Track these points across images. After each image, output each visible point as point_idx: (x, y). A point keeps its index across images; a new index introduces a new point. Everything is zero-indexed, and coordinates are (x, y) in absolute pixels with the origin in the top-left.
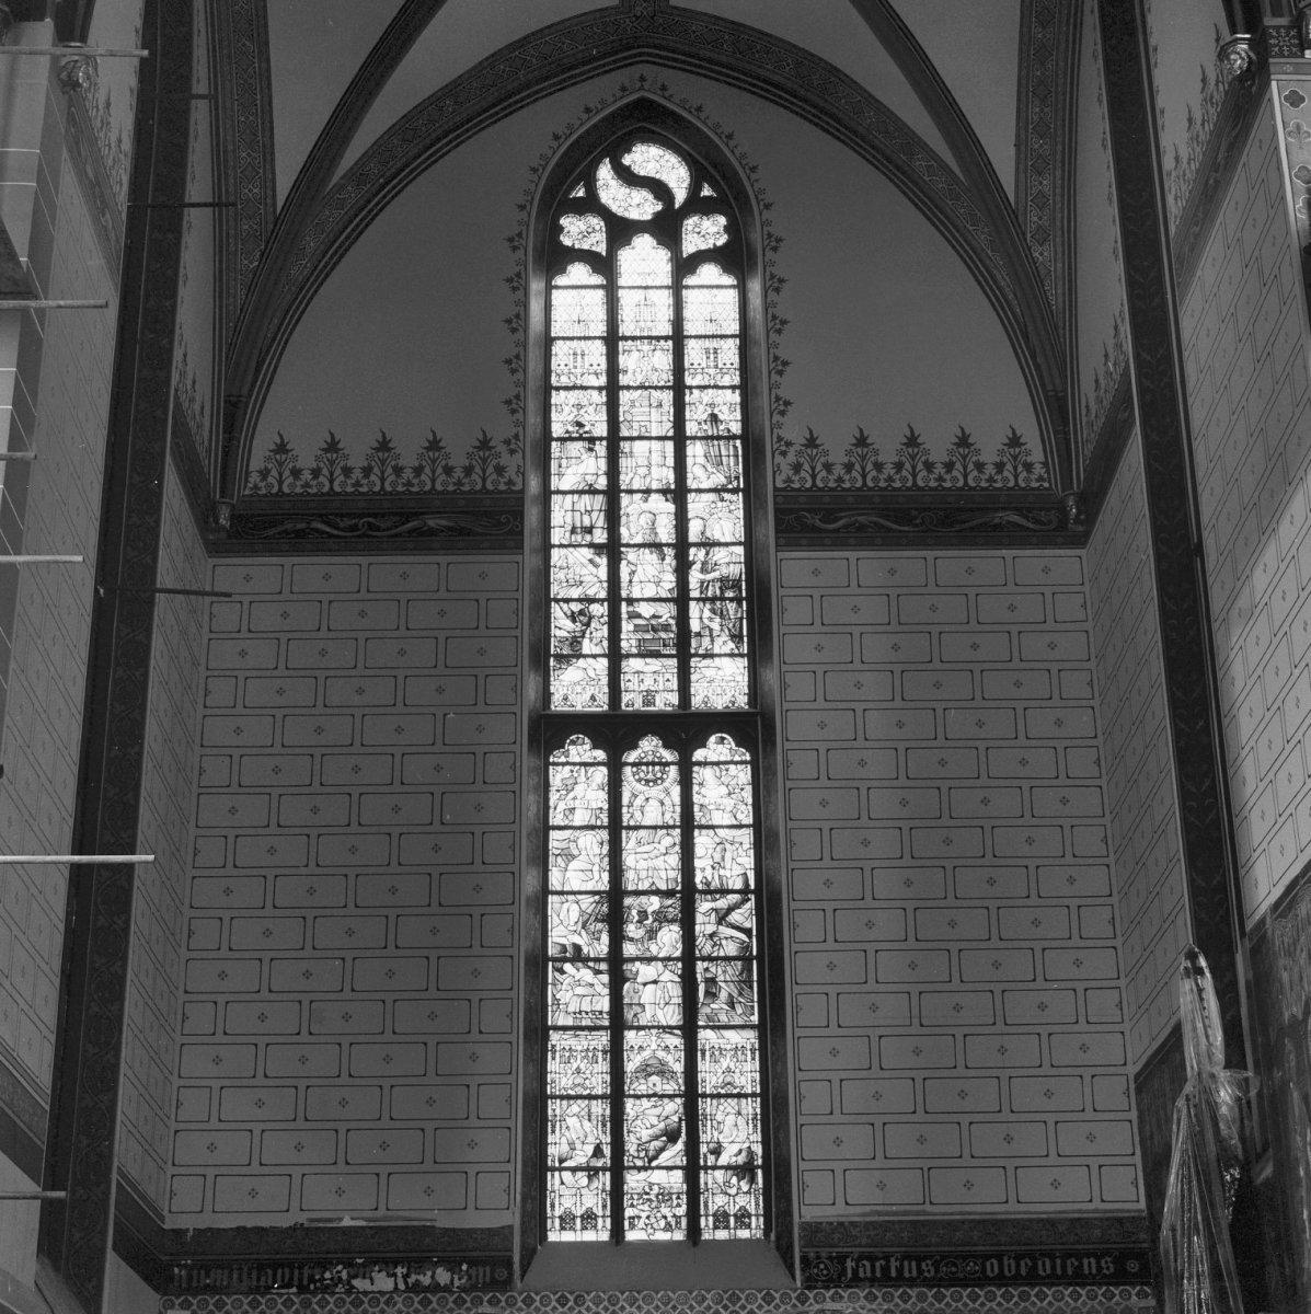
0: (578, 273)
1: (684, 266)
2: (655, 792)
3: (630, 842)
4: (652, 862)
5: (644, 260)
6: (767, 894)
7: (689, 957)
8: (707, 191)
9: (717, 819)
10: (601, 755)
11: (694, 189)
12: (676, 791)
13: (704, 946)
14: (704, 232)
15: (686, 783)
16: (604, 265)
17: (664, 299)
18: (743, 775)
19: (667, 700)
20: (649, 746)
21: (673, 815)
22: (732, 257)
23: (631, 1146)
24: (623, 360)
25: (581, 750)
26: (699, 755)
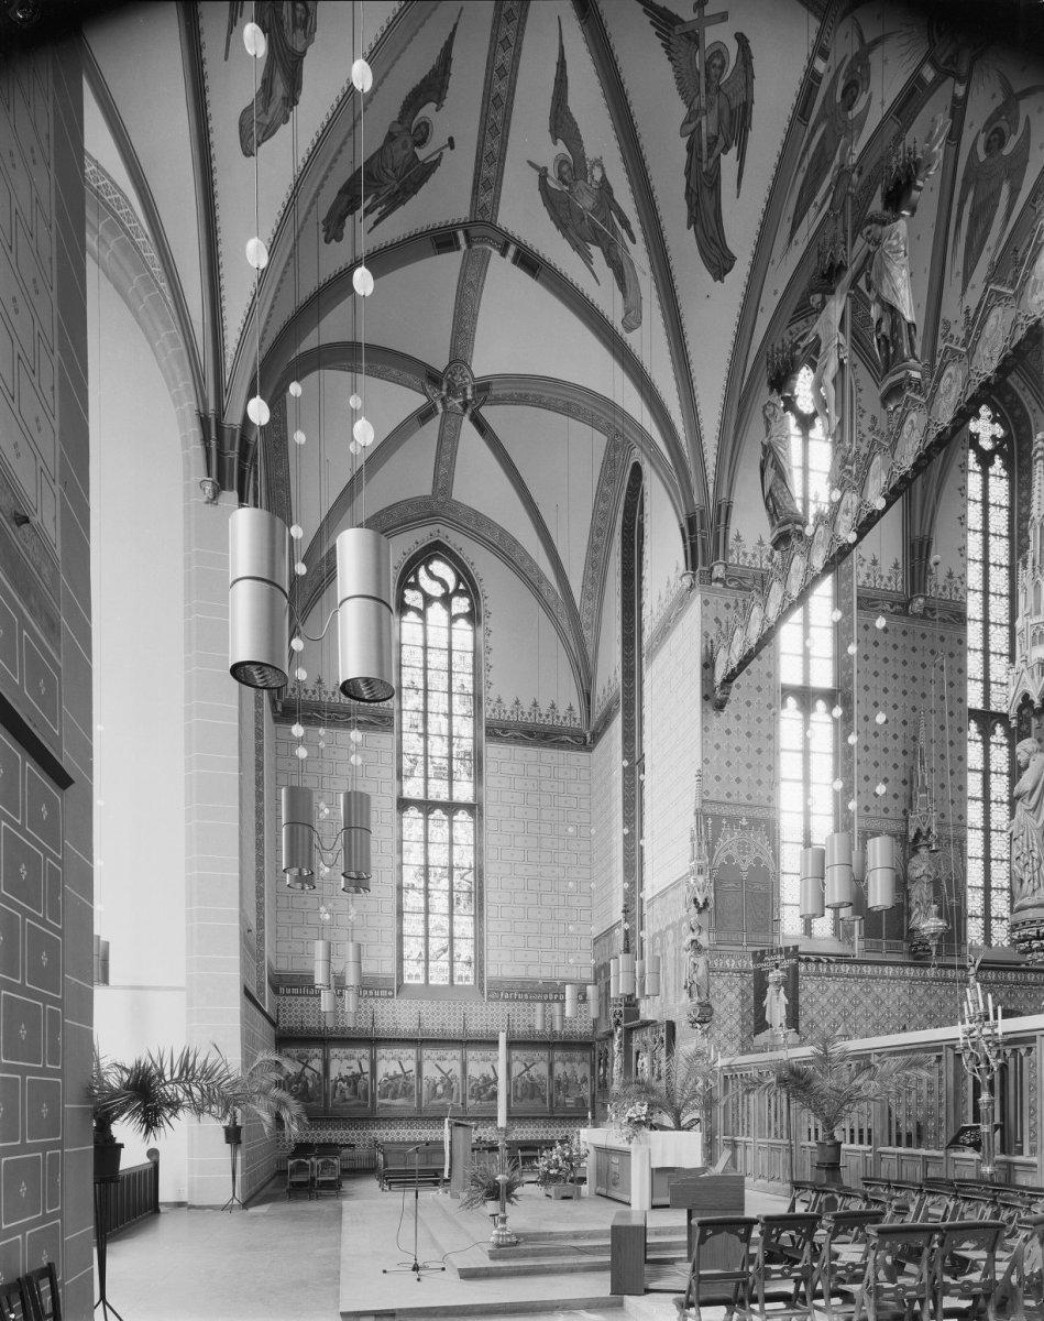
0: (411, 616)
1: (453, 619)
2: (439, 830)
3: (431, 847)
4: (438, 856)
5: (437, 613)
6: (479, 871)
7: (451, 890)
8: (462, 587)
9: (462, 842)
10: (421, 815)
11: (458, 585)
12: (447, 831)
13: (456, 887)
14: (461, 605)
15: (451, 827)
16: (422, 614)
17: (445, 632)
18: (471, 826)
19: (444, 797)
20: (438, 813)
21: (447, 839)
22: (473, 617)
23: (431, 953)
24: (429, 657)
25: (413, 812)
26: (455, 818)
